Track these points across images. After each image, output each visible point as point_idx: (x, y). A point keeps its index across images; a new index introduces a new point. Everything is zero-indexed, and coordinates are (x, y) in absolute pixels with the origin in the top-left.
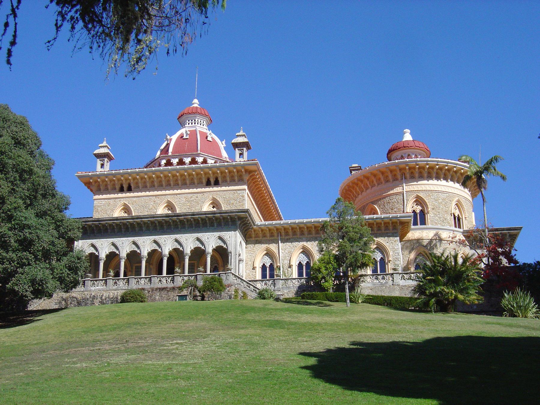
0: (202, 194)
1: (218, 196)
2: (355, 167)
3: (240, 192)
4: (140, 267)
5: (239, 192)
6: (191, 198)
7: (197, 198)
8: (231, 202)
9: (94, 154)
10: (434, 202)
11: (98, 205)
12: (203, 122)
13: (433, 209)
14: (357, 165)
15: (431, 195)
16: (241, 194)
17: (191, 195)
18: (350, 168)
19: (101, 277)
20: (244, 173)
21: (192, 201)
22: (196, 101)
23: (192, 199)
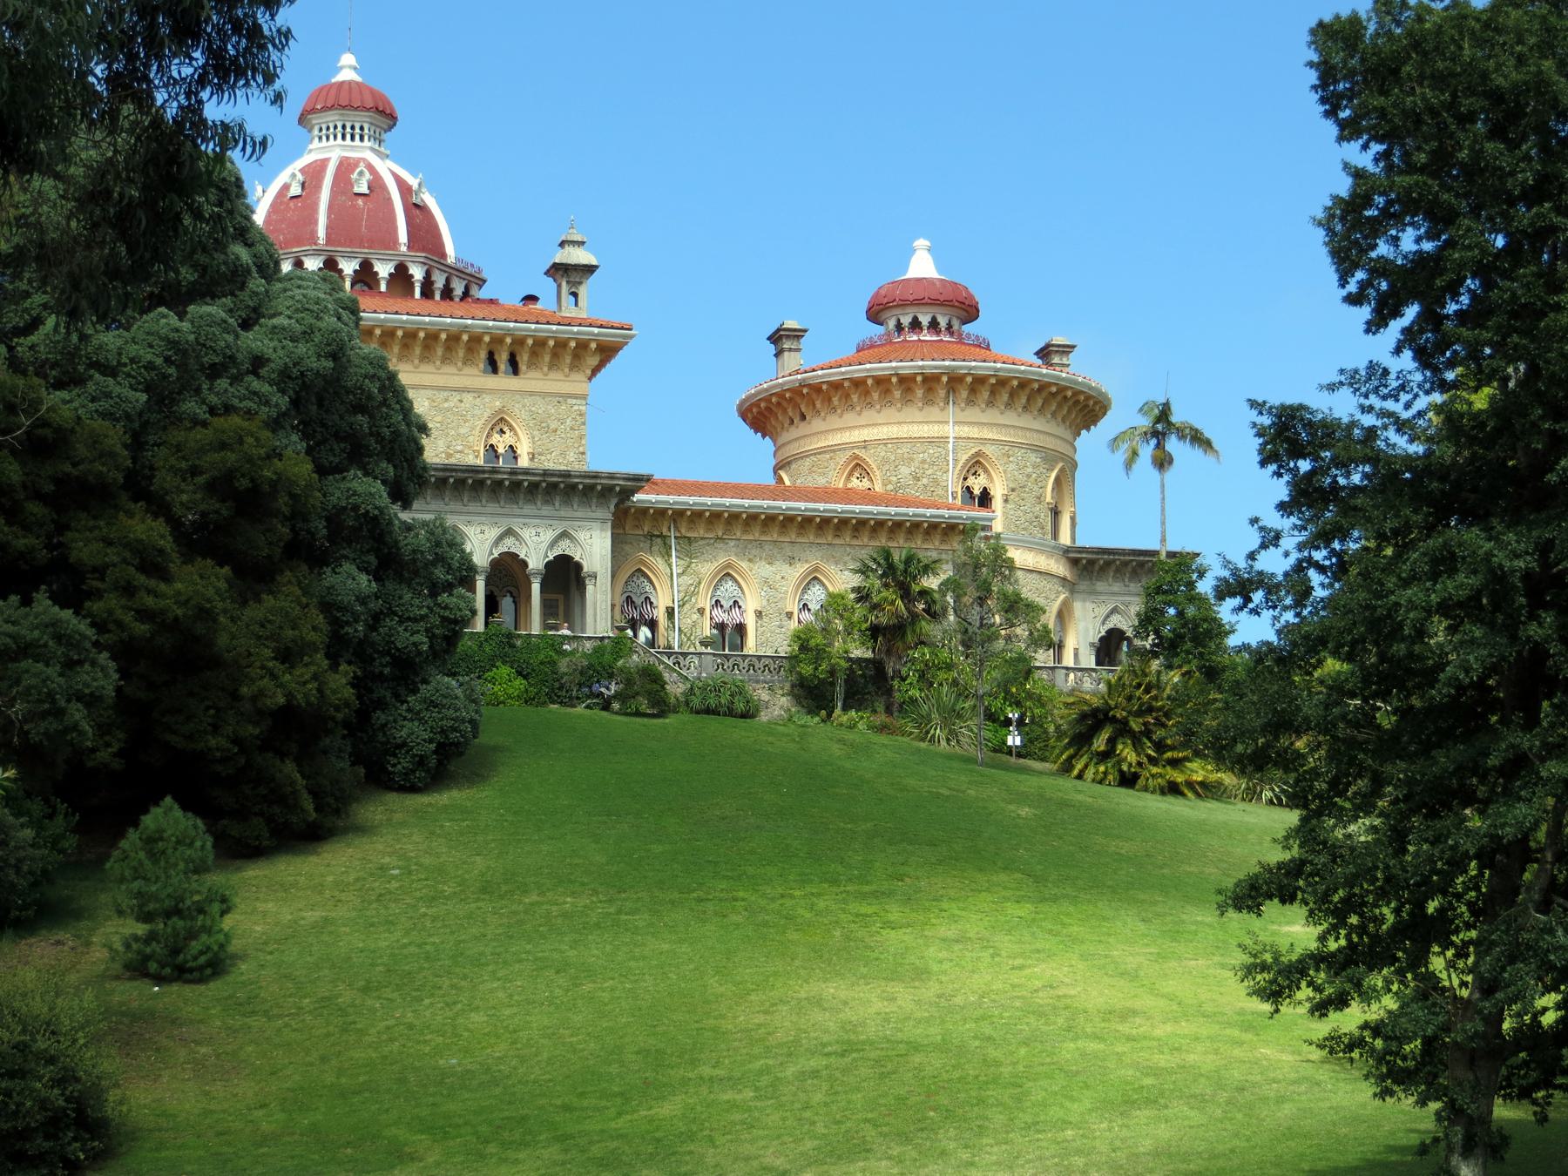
3: (574, 401)
5: (570, 401)
6: (446, 400)
7: (459, 404)
8: (553, 426)
13: (1013, 490)
16: (576, 408)
17: (446, 394)
22: (348, 59)
23: (446, 405)
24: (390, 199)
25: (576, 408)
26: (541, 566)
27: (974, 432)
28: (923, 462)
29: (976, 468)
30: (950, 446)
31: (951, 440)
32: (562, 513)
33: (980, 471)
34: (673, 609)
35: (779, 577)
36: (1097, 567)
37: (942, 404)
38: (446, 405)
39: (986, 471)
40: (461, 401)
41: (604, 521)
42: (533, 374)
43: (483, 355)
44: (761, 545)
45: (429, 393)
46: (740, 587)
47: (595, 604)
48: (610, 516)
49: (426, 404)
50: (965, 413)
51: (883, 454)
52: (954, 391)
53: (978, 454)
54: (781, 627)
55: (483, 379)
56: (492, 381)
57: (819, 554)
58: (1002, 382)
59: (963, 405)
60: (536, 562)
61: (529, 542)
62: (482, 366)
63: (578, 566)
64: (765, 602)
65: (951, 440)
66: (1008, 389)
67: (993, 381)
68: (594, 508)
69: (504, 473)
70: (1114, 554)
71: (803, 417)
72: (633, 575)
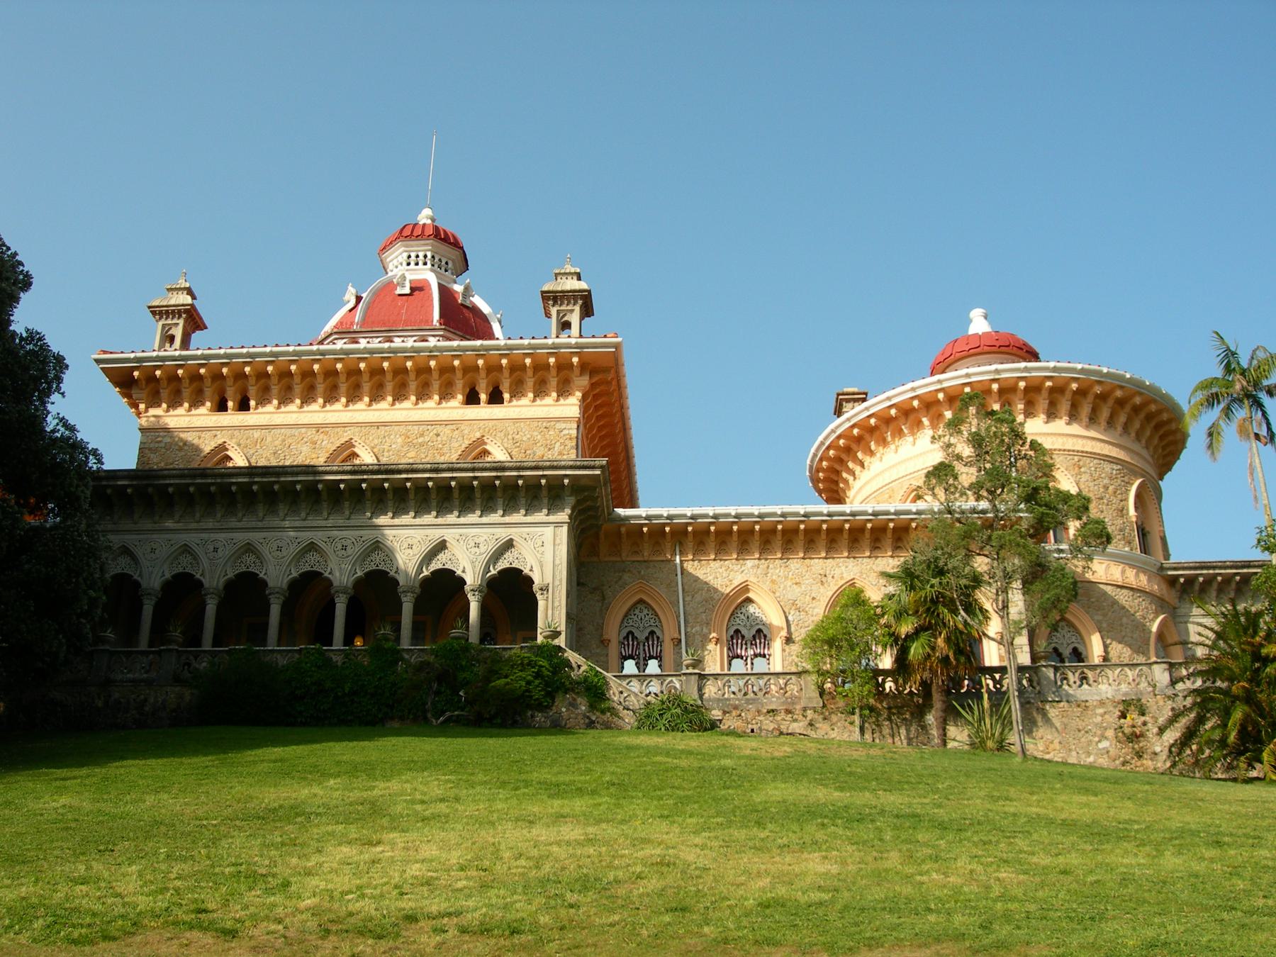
0: (454, 427)
1: (499, 434)
2: (854, 394)
3: (563, 426)
4: (265, 626)
6: (422, 435)
9: (149, 307)
10: (1091, 484)
11: (152, 446)
12: (447, 263)
14: (855, 390)
15: (1081, 463)
16: (566, 432)
18: (838, 395)
19: (143, 645)
20: (577, 371)
21: (422, 445)
22: (427, 212)
23: (420, 440)
24: (431, 294)
25: (566, 432)
34: (680, 640)
36: (1197, 587)
38: (420, 440)
40: (438, 435)
41: (558, 524)
45: (402, 429)
49: (399, 440)
55: (461, 411)
56: (473, 412)
58: (1058, 390)
60: (472, 578)
63: (530, 581)
66: (1068, 395)
67: (1049, 384)
70: (1214, 568)
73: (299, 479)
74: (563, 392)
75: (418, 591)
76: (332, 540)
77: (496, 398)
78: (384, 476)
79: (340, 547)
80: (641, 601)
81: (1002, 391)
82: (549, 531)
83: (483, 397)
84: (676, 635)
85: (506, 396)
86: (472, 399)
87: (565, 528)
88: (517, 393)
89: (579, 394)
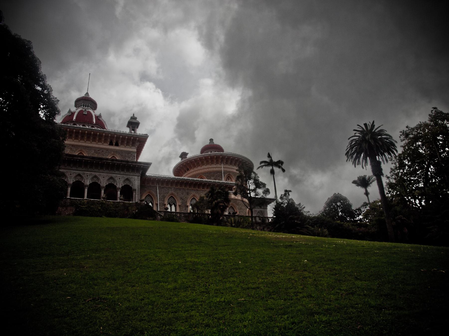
5: (131, 153)
6: (99, 151)
21: (99, 153)
26: (120, 187)
27: (228, 170)
28: (217, 176)
29: (229, 178)
30: (223, 172)
31: (223, 171)
32: (127, 174)
33: (229, 179)
34: (158, 204)
35: (185, 197)
37: (220, 163)
38: (99, 152)
39: (231, 178)
40: (103, 151)
41: (138, 176)
42: (122, 146)
43: (109, 140)
44: (180, 189)
46: (175, 200)
47: (135, 198)
48: (140, 175)
49: (93, 151)
50: (225, 166)
51: (207, 175)
52: (223, 161)
53: (229, 175)
54: (185, 209)
55: (109, 146)
57: (194, 192)
59: (225, 164)
61: (117, 181)
62: (109, 143)
63: (131, 188)
64: (181, 203)
65: (223, 171)
68: (135, 172)
69: (109, 160)
71: (188, 170)
72: (147, 196)
73: (79, 158)
74: (133, 145)
75: (105, 188)
76: (84, 174)
77: (117, 145)
78: (89, 159)
79: (86, 175)
80: (149, 195)
81: (216, 158)
82: (136, 177)
83: (114, 144)
84: (157, 203)
85: (120, 144)
86: (111, 144)
87: (140, 177)
88: (122, 143)
89: (136, 146)
